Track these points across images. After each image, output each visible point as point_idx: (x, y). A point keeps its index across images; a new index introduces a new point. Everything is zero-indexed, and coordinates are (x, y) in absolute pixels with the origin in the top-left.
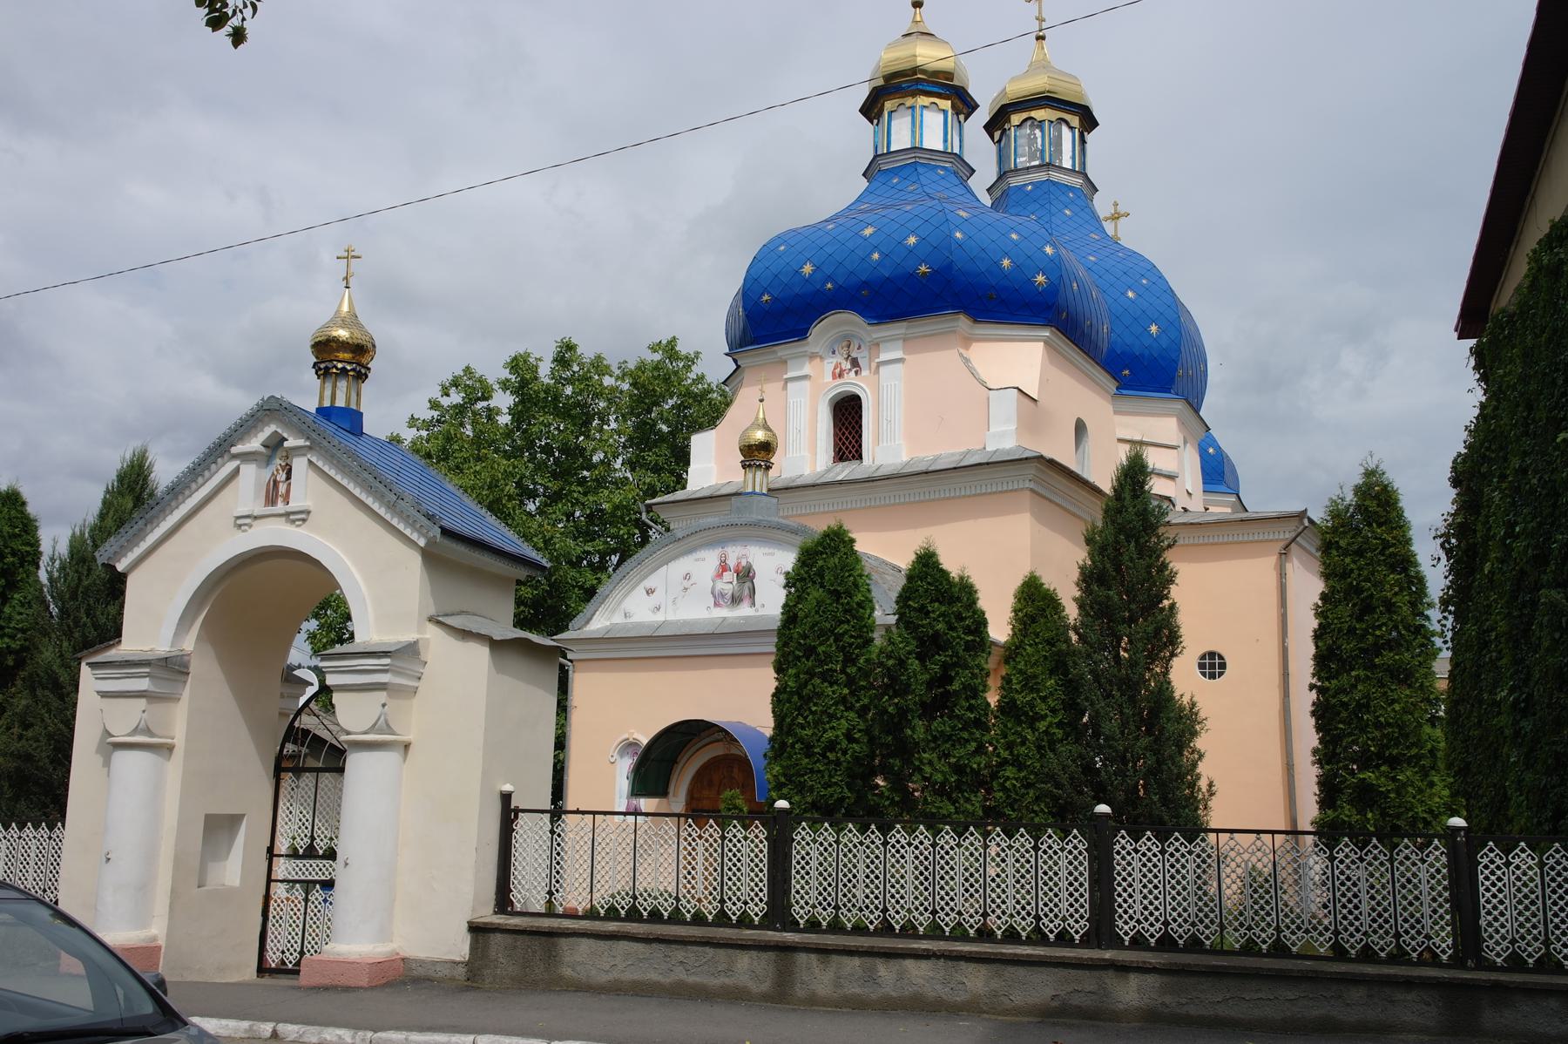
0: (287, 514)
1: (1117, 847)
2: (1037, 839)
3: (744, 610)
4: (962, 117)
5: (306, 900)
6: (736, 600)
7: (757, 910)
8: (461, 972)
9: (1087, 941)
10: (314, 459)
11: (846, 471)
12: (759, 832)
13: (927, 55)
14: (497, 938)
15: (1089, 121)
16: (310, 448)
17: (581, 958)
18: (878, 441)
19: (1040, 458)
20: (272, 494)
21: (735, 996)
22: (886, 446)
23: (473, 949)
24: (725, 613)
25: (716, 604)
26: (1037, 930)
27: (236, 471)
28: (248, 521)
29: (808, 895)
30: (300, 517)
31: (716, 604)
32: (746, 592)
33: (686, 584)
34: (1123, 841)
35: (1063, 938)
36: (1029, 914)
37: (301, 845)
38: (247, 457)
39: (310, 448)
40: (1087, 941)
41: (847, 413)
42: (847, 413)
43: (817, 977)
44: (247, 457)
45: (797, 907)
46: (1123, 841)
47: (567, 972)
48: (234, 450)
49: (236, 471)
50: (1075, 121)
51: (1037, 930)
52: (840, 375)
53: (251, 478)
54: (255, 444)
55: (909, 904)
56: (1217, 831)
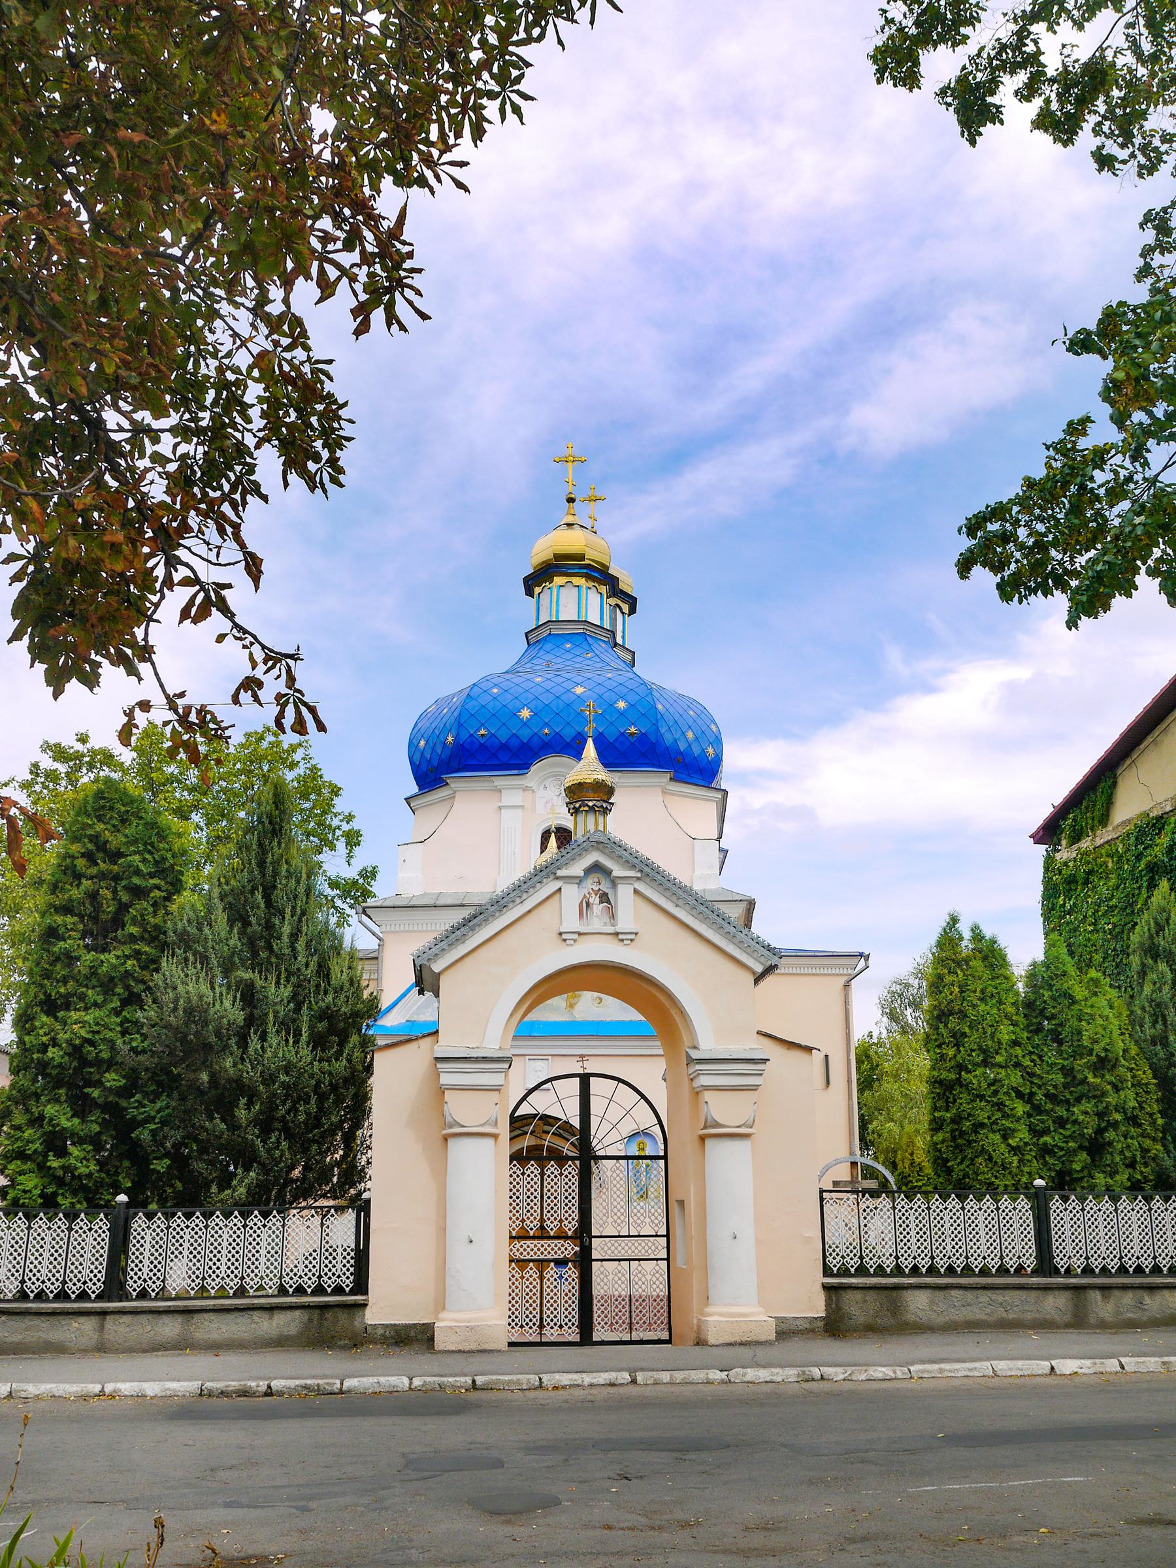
0: (617, 934)
2: (997, 1201)
5: (542, 1278)
7: (1030, 1262)
8: (821, 1324)
9: (1035, 1272)
10: (641, 887)
12: (1024, 1203)
14: (850, 1296)
15: (633, 610)
17: (918, 1303)
21: (1044, 1325)
23: (828, 1305)
26: (898, 1266)
28: (575, 936)
29: (1068, 1250)
34: (1055, 1204)
35: (339, 1290)
37: (532, 1225)
39: (638, 879)
40: (1035, 1272)
43: (1101, 1307)
45: (131, 1282)
47: (910, 1317)
48: (560, 873)
50: (625, 608)
51: (898, 1266)
53: (572, 895)
55: (1137, 1252)
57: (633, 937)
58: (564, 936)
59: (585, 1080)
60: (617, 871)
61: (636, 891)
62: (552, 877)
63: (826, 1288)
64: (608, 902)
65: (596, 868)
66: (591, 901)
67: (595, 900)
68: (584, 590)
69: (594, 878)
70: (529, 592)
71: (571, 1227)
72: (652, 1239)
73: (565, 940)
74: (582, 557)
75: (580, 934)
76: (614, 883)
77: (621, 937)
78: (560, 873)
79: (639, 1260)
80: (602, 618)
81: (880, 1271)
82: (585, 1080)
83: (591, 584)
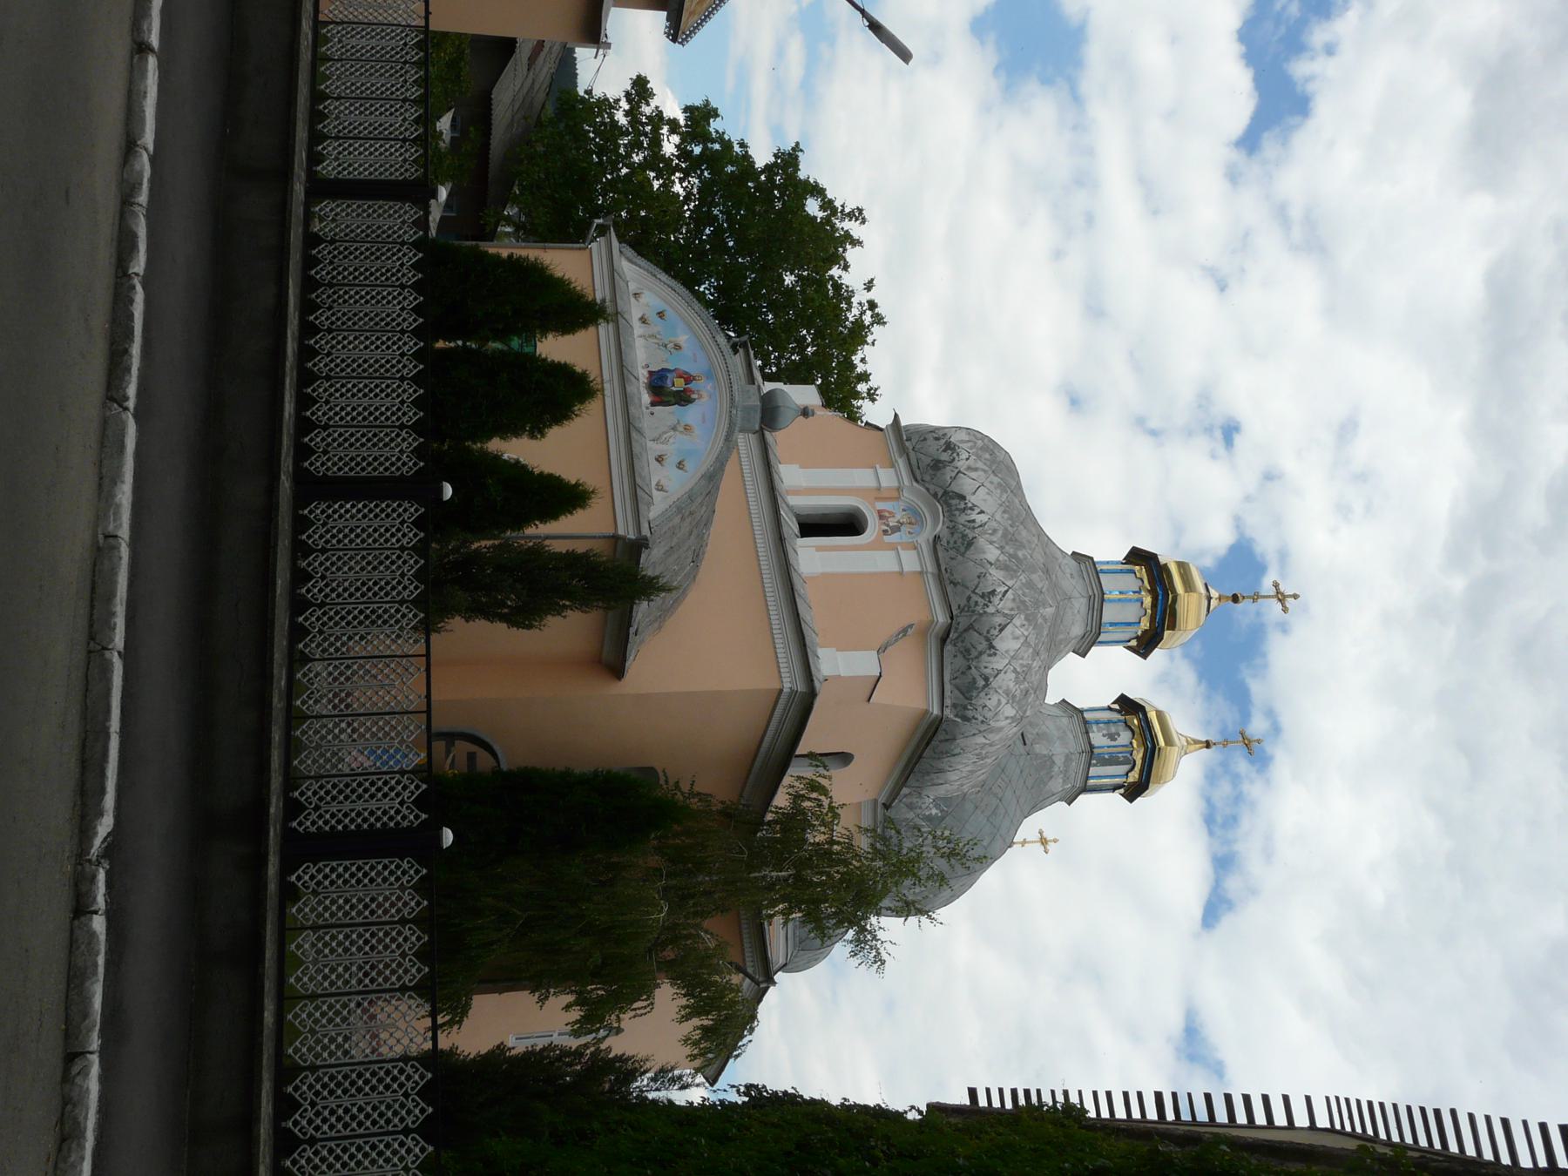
1: (406, 504)
3: (646, 398)
4: (1134, 643)
11: (791, 526)
13: (1190, 607)
18: (819, 549)
19: (812, 694)
22: (814, 558)
24: (643, 375)
25: (651, 373)
31: (651, 373)
33: (670, 346)
36: (326, 596)
41: (847, 525)
42: (847, 525)
46: (412, 510)
52: (881, 517)
56: (428, 641)
74: (1173, 627)
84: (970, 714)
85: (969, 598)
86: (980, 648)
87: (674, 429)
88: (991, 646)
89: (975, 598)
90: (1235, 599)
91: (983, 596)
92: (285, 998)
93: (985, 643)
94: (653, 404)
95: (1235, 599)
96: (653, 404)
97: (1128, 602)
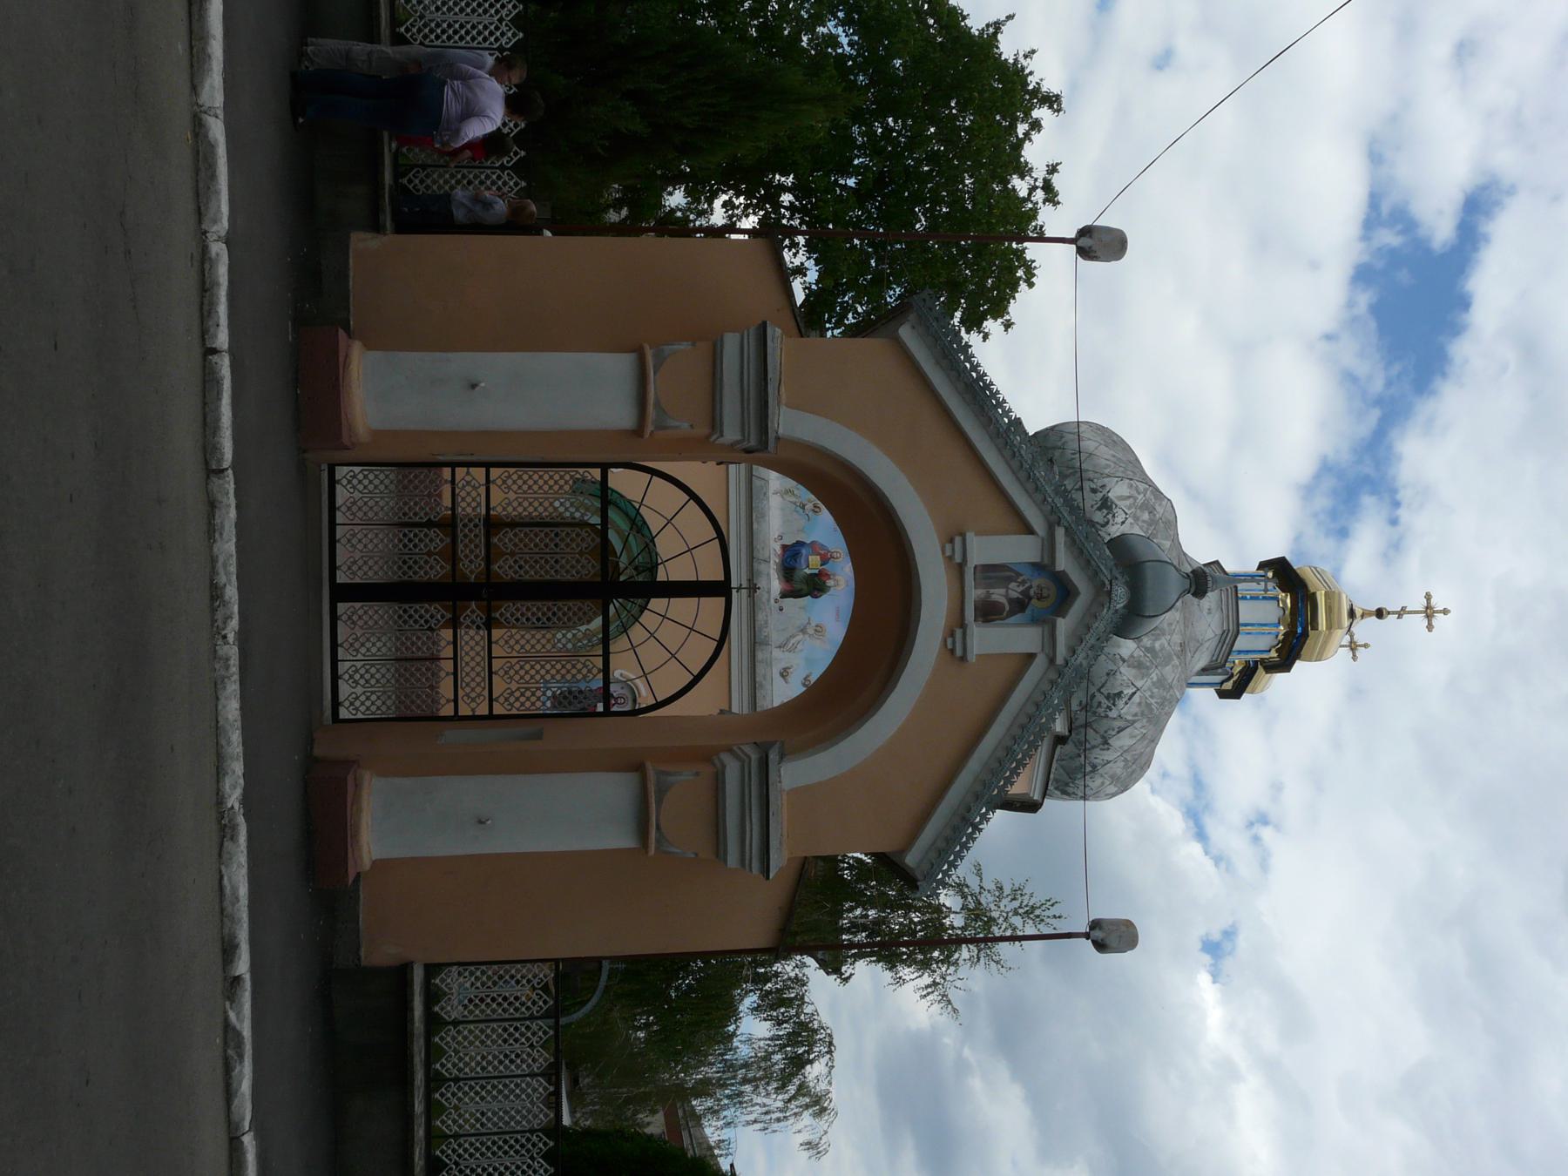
3: (776, 585)
6: (788, 570)
15: (1223, 694)
16: (1052, 661)
20: (993, 573)
25: (784, 547)
27: (1029, 530)
28: (958, 559)
30: (954, 654)
31: (784, 547)
32: (798, 586)
38: (1050, 546)
39: (1052, 661)
44: (1050, 546)
48: (1060, 533)
49: (1029, 530)
54: (1063, 562)
57: (959, 652)
58: (958, 540)
59: (721, 589)
60: (1063, 625)
61: (1031, 657)
62: (1053, 518)
63: (404, 970)
64: (1012, 613)
65: (1065, 593)
66: (1013, 585)
67: (1015, 590)
68: (1274, 630)
69: (1051, 591)
70: (1263, 565)
71: (505, 570)
72: (486, 693)
73: (952, 541)
75: (961, 568)
76: (1046, 621)
77: (959, 633)
78: (1060, 533)
79: (455, 674)
80: (1240, 652)
81: (433, 1053)
82: (721, 589)
83: (1281, 637)
84: (1070, 790)
85: (1093, 696)
86: (1094, 743)
87: (803, 631)
88: (1106, 742)
89: (1099, 697)
90: (1380, 613)
91: (1108, 697)
92: (435, 1081)
93: (1100, 740)
94: (784, 595)
95: (1380, 613)
96: (784, 595)
97: (1264, 615)
